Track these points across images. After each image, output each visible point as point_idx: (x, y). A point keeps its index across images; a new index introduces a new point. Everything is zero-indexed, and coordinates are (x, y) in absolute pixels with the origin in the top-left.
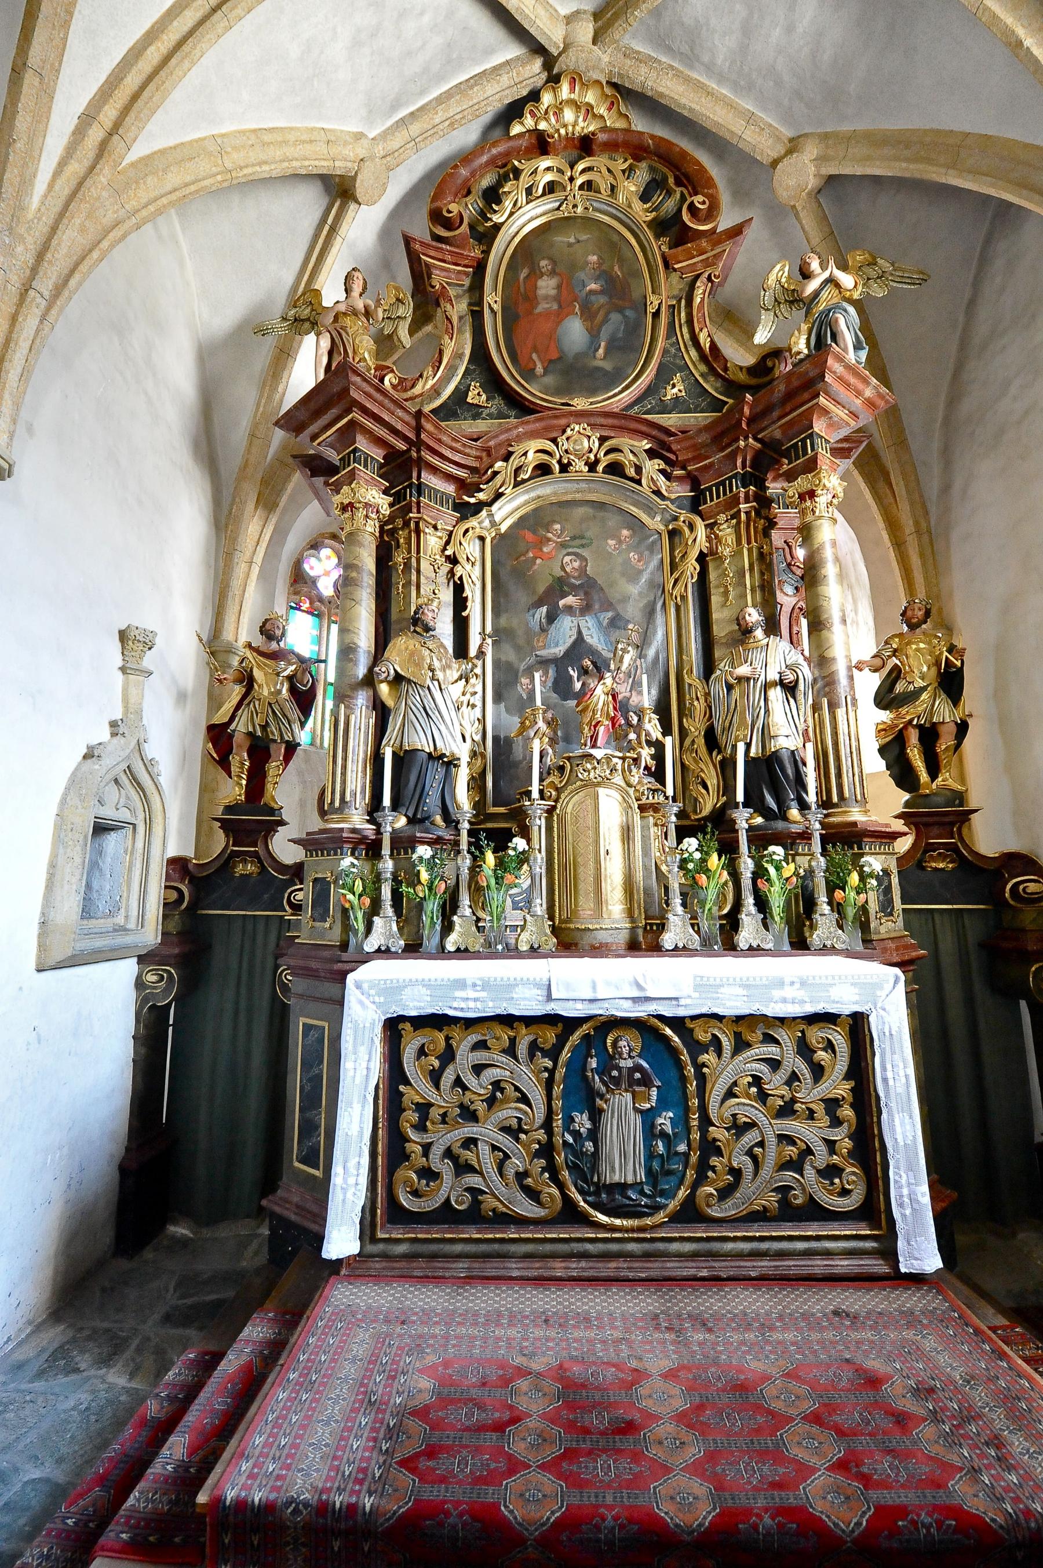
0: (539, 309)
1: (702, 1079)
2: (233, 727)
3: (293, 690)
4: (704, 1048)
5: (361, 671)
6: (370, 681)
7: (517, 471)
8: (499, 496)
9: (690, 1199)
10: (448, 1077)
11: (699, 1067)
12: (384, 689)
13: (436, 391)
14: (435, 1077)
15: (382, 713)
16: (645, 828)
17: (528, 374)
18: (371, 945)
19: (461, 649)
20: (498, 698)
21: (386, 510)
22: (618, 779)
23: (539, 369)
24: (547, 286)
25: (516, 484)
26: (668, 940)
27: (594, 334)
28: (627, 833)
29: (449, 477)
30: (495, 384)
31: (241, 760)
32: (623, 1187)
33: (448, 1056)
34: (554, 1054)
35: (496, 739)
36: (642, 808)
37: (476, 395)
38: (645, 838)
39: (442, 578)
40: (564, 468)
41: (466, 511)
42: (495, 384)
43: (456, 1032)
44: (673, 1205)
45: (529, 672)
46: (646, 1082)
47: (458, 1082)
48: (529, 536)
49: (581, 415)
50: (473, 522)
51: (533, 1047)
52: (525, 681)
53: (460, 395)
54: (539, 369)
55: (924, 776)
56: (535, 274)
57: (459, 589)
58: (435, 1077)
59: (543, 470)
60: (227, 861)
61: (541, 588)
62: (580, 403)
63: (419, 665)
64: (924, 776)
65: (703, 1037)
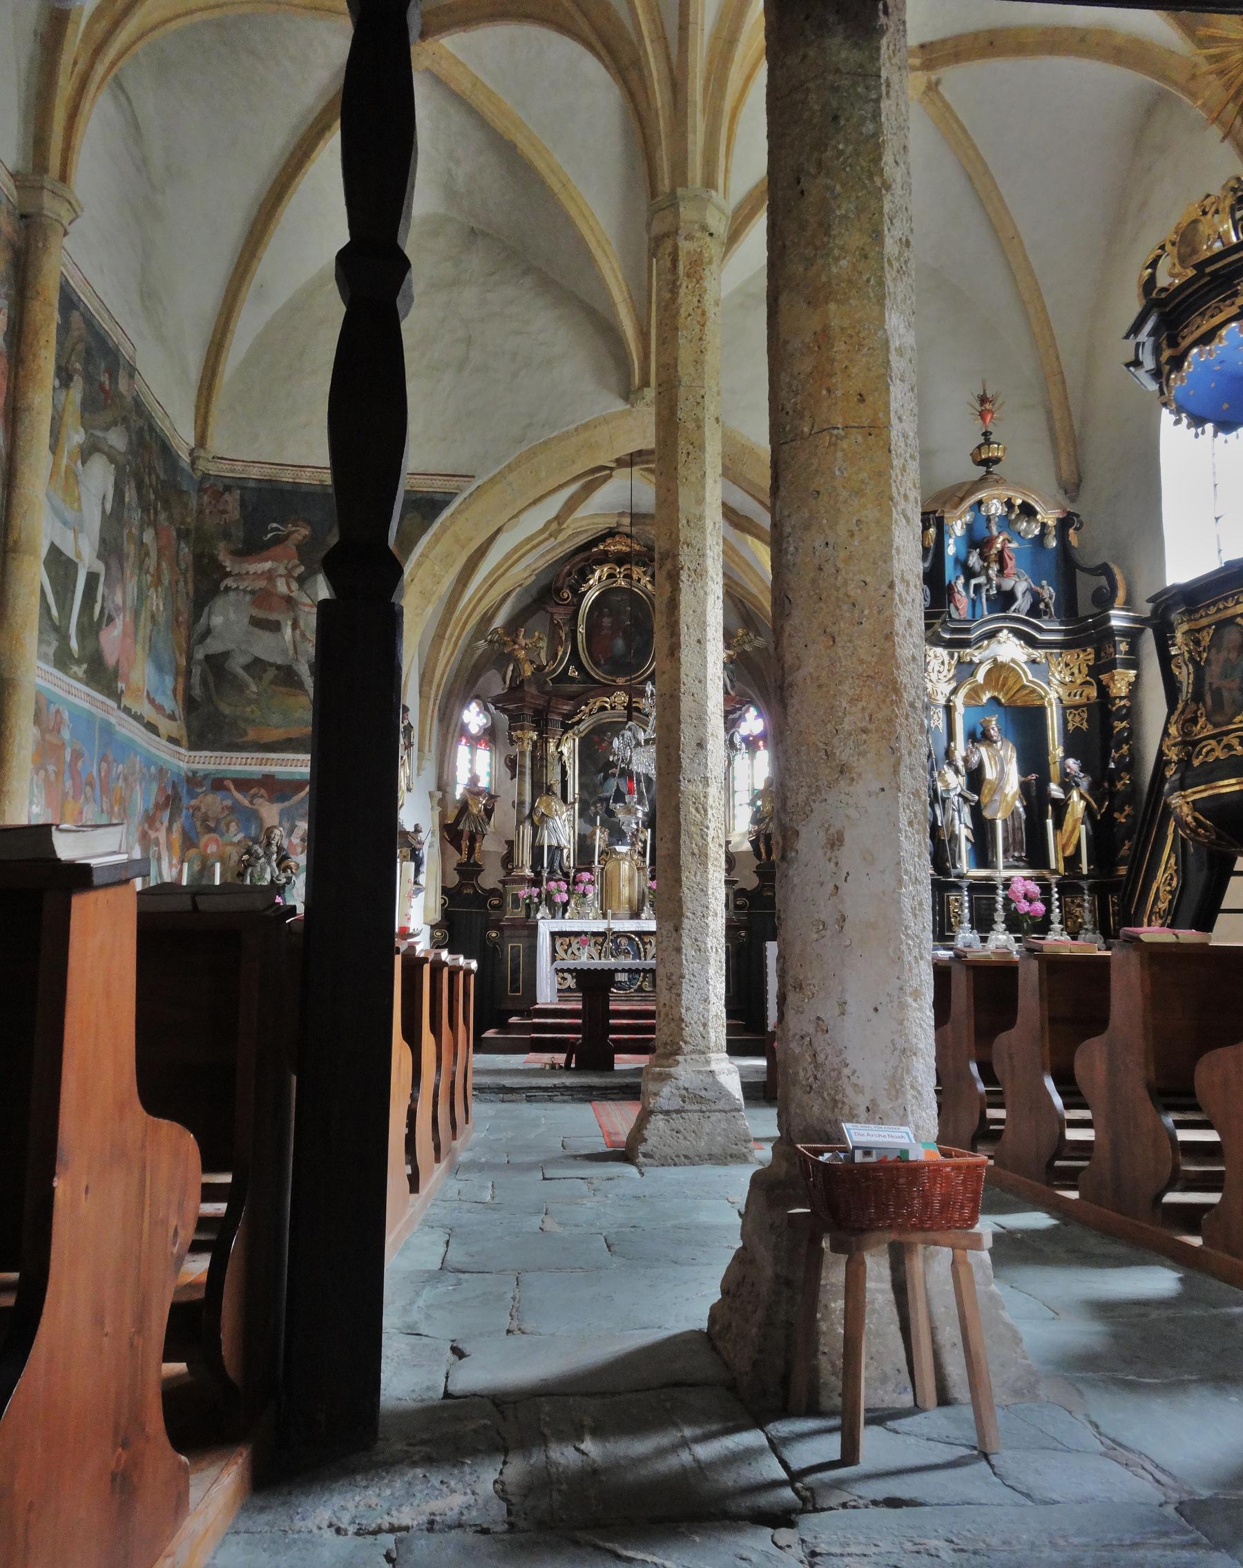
0: (603, 633)
1: (645, 952)
2: (461, 827)
3: (485, 809)
4: (646, 943)
5: (527, 812)
6: (530, 816)
7: (591, 710)
8: (581, 721)
9: (640, 987)
10: (570, 951)
11: (645, 949)
12: (536, 818)
13: (554, 670)
14: (566, 951)
15: (536, 829)
16: (639, 876)
17: (597, 664)
18: (539, 916)
19: (564, 798)
20: (580, 816)
21: (535, 738)
22: (629, 858)
23: (602, 662)
24: (606, 621)
25: (590, 715)
26: (643, 916)
27: (628, 646)
28: (631, 880)
29: (559, 714)
30: (580, 667)
31: (465, 844)
32: (621, 982)
33: (570, 945)
34: (602, 945)
35: (579, 834)
36: (638, 869)
37: (573, 672)
38: (639, 880)
39: (556, 762)
40: (613, 708)
41: (567, 728)
42: (580, 667)
43: (572, 938)
44: (636, 987)
45: (595, 804)
46: (629, 953)
47: (573, 953)
48: (596, 738)
49: (620, 688)
50: (570, 733)
51: (596, 943)
52: (592, 808)
53: (566, 669)
54: (602, 662)
55: (764, 855)
56: (601, 615)
57: (563, 767)
58: (566, 951)
59: (604, 708)
60: (460, 886)
61: (601, 765)
62: (621, 681)
63: (551, 810)
64: (764, 855)
65: (646, 940)
